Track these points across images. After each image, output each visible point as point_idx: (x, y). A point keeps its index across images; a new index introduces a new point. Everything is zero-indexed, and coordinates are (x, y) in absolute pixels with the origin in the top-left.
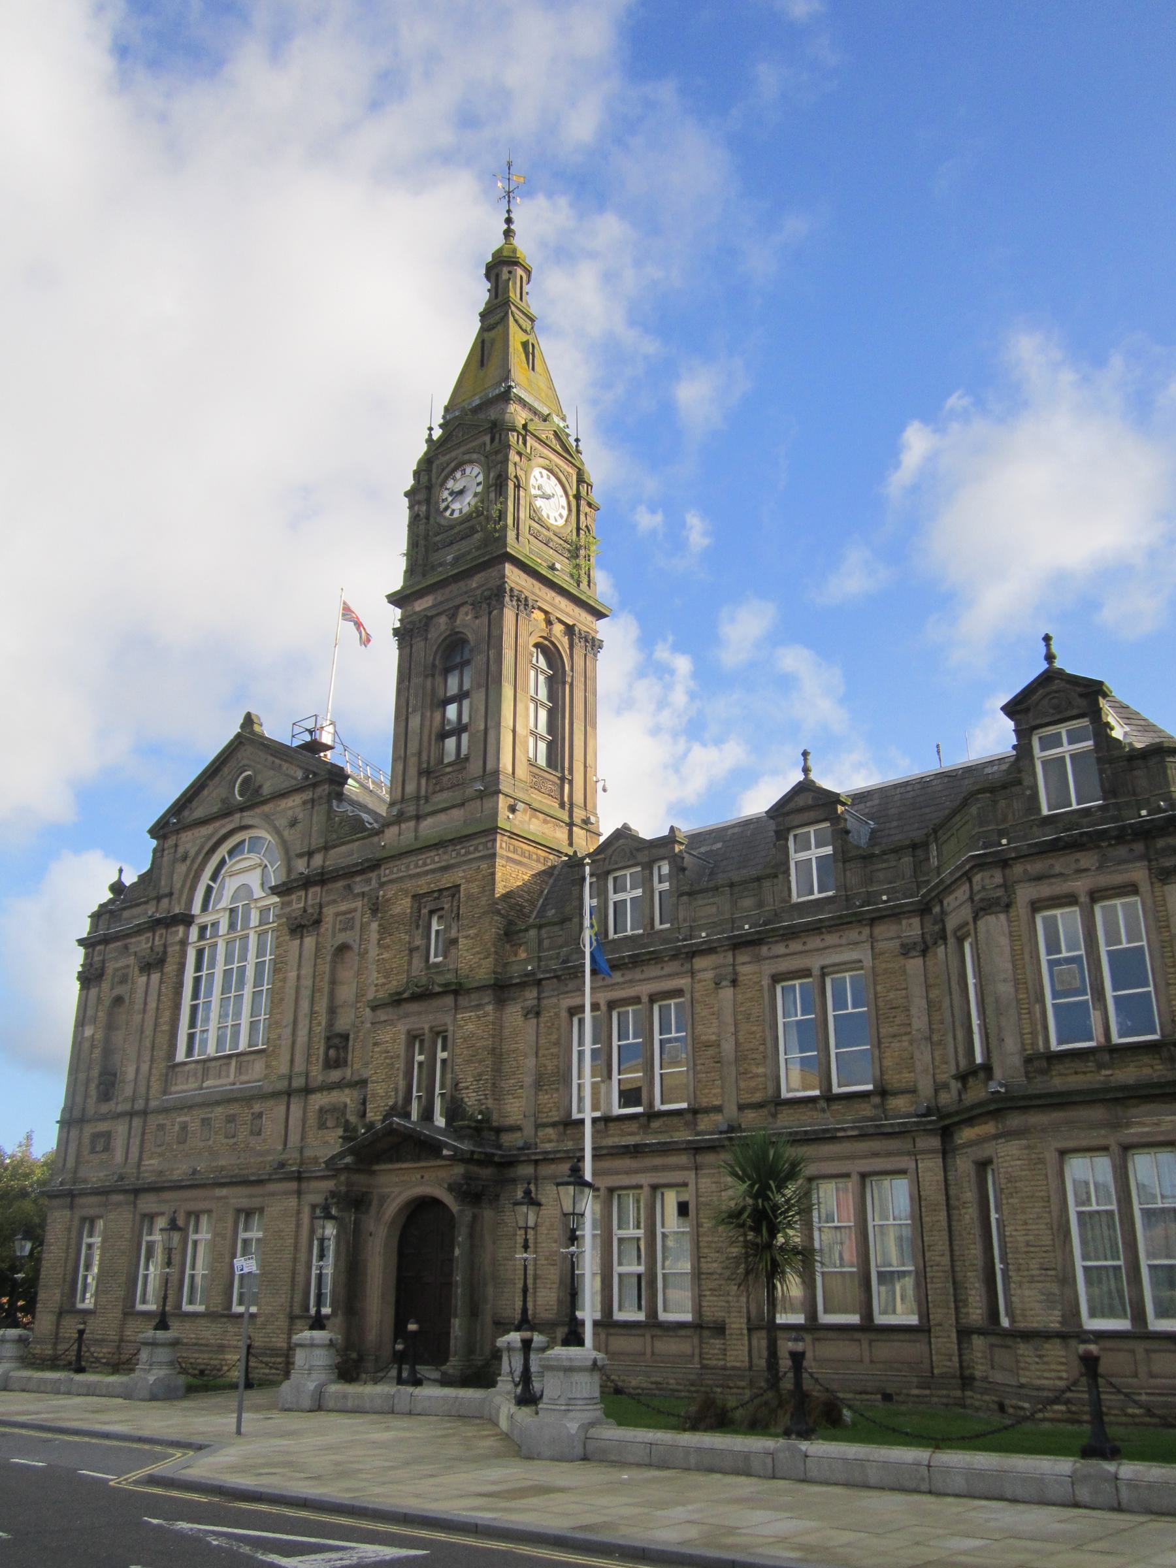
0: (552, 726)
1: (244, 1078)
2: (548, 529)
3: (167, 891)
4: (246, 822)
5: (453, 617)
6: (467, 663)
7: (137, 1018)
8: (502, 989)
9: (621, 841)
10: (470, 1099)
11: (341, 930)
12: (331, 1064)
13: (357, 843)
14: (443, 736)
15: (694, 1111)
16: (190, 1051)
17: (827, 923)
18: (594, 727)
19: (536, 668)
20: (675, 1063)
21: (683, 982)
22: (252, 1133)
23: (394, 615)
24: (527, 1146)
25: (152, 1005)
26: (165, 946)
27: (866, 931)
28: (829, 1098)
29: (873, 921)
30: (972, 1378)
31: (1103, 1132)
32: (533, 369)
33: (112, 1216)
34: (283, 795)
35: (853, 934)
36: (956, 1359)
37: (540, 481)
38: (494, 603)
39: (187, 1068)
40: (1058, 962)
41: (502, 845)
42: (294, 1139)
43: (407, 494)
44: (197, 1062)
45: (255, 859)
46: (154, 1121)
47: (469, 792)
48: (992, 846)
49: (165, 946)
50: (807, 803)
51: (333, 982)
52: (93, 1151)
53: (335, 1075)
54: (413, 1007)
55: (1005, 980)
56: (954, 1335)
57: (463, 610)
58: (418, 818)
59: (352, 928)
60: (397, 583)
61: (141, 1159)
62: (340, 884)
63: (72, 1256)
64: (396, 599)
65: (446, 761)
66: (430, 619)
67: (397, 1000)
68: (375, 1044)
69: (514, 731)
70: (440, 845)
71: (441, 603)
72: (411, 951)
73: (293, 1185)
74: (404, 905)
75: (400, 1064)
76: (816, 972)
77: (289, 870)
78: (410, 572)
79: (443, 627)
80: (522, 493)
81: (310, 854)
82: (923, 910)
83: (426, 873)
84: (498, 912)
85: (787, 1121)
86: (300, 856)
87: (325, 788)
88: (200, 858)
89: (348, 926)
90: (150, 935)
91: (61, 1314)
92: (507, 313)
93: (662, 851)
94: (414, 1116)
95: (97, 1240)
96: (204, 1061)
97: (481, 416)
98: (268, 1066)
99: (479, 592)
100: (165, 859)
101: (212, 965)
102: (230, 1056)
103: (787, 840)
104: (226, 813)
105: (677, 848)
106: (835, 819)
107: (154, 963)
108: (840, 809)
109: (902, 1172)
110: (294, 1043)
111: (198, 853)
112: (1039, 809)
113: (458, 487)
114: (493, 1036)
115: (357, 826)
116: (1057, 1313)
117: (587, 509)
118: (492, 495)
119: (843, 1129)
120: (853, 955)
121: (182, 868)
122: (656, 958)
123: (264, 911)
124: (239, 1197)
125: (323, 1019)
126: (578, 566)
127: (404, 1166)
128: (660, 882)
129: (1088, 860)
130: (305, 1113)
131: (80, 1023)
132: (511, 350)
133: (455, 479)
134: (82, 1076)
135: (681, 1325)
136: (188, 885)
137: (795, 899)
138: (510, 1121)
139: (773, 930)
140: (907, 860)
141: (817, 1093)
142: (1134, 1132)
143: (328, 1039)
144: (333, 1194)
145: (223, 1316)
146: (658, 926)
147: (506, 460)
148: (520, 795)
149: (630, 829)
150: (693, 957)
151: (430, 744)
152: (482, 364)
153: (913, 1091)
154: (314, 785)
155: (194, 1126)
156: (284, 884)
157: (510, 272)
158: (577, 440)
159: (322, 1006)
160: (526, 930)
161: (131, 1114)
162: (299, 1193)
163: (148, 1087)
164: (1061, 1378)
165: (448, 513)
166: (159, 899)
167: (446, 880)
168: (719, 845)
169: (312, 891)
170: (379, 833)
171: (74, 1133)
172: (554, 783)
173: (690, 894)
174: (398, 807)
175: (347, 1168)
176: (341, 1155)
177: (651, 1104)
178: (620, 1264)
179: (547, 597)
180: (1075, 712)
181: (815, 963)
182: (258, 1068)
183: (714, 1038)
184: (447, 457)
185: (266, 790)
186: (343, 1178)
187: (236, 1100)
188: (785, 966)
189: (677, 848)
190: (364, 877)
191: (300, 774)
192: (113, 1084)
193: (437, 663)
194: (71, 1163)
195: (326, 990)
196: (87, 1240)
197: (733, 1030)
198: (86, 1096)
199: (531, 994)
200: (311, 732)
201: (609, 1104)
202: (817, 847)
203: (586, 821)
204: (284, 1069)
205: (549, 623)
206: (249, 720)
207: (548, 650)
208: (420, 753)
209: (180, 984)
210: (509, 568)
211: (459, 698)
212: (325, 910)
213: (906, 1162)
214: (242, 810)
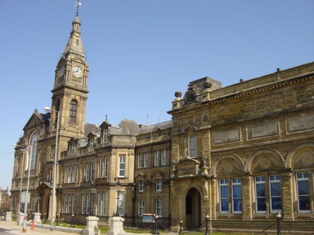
23: (52, 94)
34: (39, 125)
60: (52, 89)
64: (52, 91)
117: (87, 72)
205: (75, 96)
206: (35, 111)
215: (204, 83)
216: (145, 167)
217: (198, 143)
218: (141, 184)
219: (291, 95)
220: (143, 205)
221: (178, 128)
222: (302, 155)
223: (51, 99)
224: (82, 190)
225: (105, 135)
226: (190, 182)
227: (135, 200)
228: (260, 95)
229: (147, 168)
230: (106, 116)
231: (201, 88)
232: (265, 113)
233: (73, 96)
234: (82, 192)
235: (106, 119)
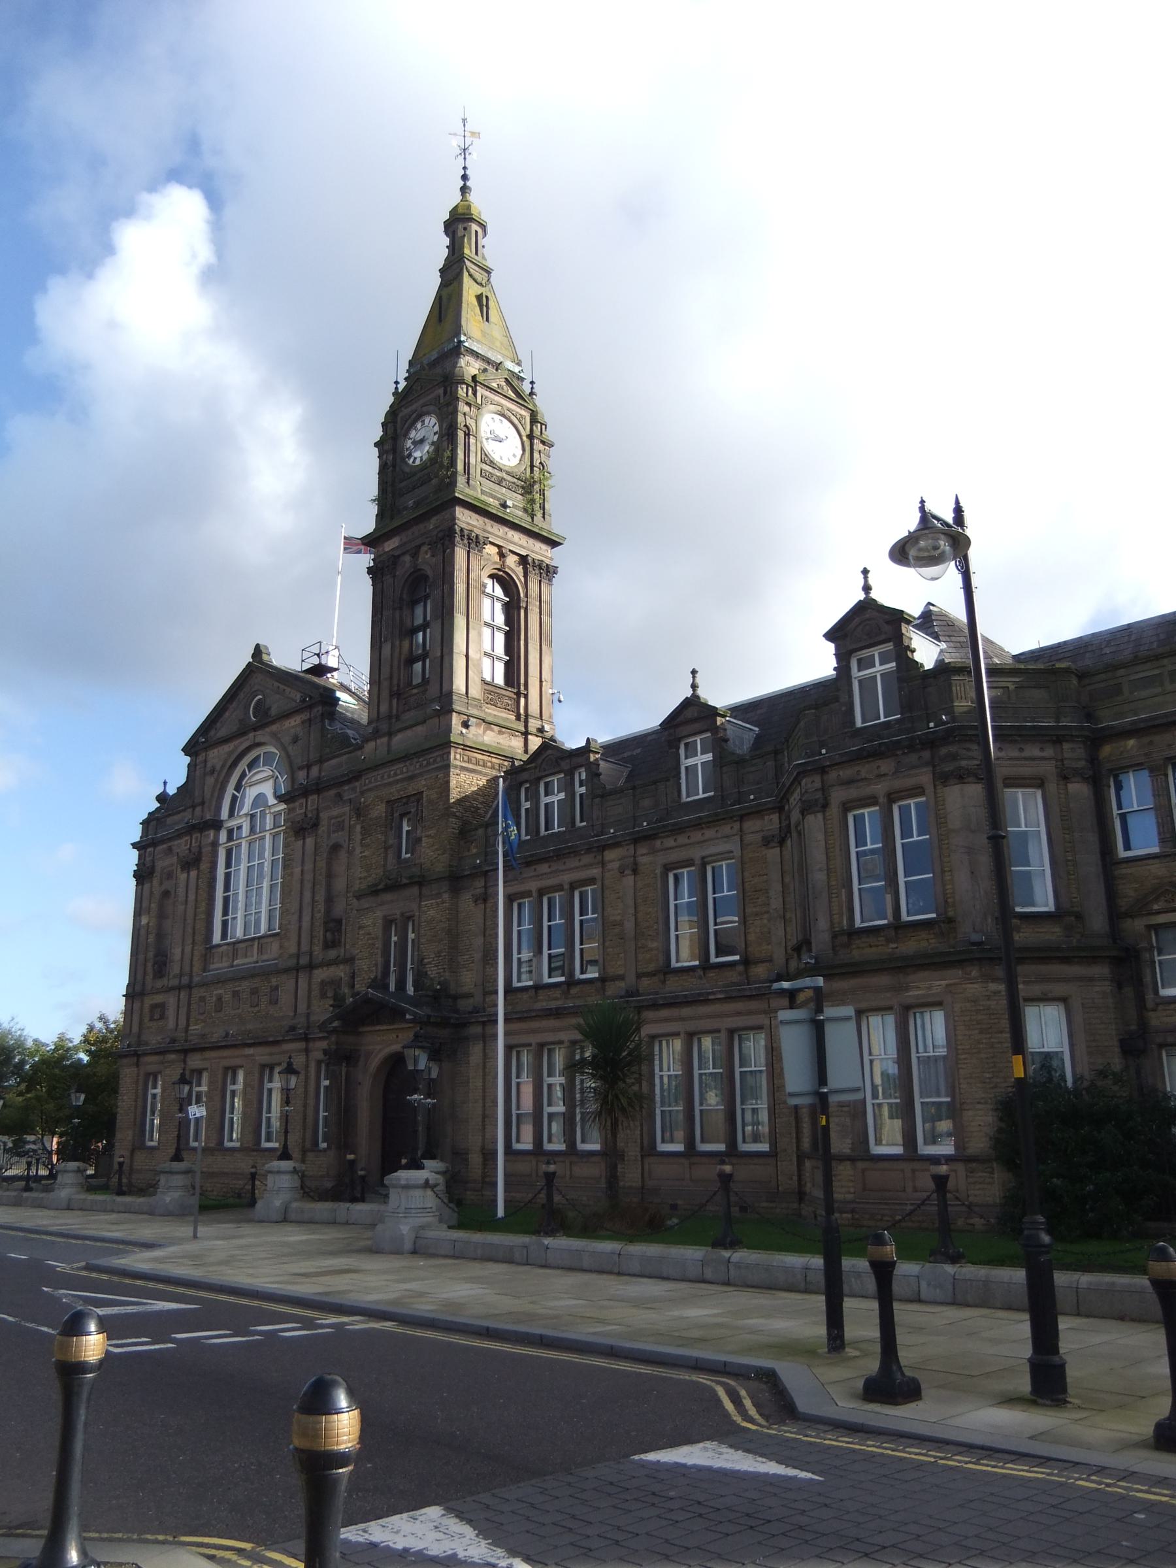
1: (265, 957)
2: (501, 470)
3: (198, 800)
4: (259, 739)
5: (415, 555)
6: (427, 597)
7: (181, 908)
8: (456, 880)
9: (549, 752)
10: (432, 971)
11: (334, 832)
12: (328, 945)
13: (345, 757)
14: (411, 661)
15: (603, 980)
16: (224, 935)
17: (705, 820)
18: (550, 645)
19: (492, 597)
20: (591, 939)
21: (595, 872)
22: (271, 1003)
24: (476, 1010)
25: (192, 897)
26: (200, 847)
27: (737, 826)
28: (706, 966)
29: (742, 818)
30: (805, 1193)
31: (888, 995)
32: (487, 320)
33: (168, 1071)
34: (287, 715)
35: (726, 829)
36: (795, 1178)
37: (493, 426)
38: (447, 543)
39: (221, 949)
40: (865, 853)
41: (456, 757)
42: (302, 1007)
43: (376, 445)
44: (228, 944)
45: (267, 772)
46: (197, 993)
47: (429, 711)
48: (813, 755)
49: (200, 847)
50: (693, 715)
52: (152, 1019)
53: (332, 954)
54: (388, 897)
55: (820, 870)
56: (795, 1159)
57: (425, 548)
58: (390, 734)
59: (343, 829)
61: (188, 1025)
62: (332, 792)
63: (140, 1103)
64: (370, 542)
65: (415, 682)
66: (399, 556)
67: (374, 891)
68: (360, 928)
69: (467, 656)
70: (406, 757)
71: (405, 543)
72: (386, 849)
73: (302, 1045)
74: (379, 810)
75: (379, 944)
76: (698, 862)
77: (293, 779)
78: (380, 517)
79: (408, 565)
80: (472, 440)
81: (308, 767)
82: (780, 809)
83: (397, 782)
84: (454, 815)
85: (673, 986)
86: (301, 768)
88: (225, 771)
89: (340, 827)
90: (188, 838)
91: (132, 1152)
92: (462, 270)
93: (580, 760)
94: (392, 987)
95: (158, 1091)
96: (234, 943)
97: (438, 370)
98: (281, 947)
99: (435, 533)
100: (198, 773)
101: (238, 863)
102: (253, 939)
103: (678, 748)
104: (241, 733)
105: (592, 757)
106: (715, 729)
107: (191, 862)
108: (719, 720)
109: (759, 1028)
110: (300, 928)
111: (223, 766)
112: (853, 722)
113: (419, 437)
114: (449, 920)
115: (344, 741)
116: (849, 1141)
118: (445, 444)
119: (713, 993)
120: (722, 847)
121: (210, 781)
122: (574, 852)
123: (276, 816)
124: (261, 1055)
125: (321, 907)
127: (385, 1027)
128: (581, 786)
130: (310, 984)
131: (138, 913)
132: (464, 305)
133: (416, 429)
134: (141, 957)
135: (592, 1153)
136: (216, 794)
137: (684, 799)
138: (465, 989)
139: (664, 826)
140: (771, 763)
141: (697, 963)
143: (325, 923)
144: (325, 1052)
145: (254, 1150)
146: (578, 824)
147: (456, 411)
149: (555, 741)
150: (603, 850)
151: (399, 667)
152: (440, 320)
153: (771, 961)
154: (310, 707)
155: (227, 997)
156: (287, 793)
157: (465, 229)
158: (532, 383)
159: (321, 897)
160: (476, 829)
161: (179, 988)
162: (307, 1051)
163: (192, 965)
164: (849, 1193)
165: (411, 461)
166: (194, 807)
167: (411, 791)
168: (639, 751)
169: (310, 798)
170: (360, 747)
171: (137, 1005)
172: (510, 698)
173: (602, 796)
174: (374, 725)
175: (335, 1030)
176: (330, 1020)
177: (571, 973)
178: (549, 1105)
179: (498, 532)
180: (883, 637)
181: (697, 854)
182: (274, 948)
183: (618, 918)
184: (409, 409)
185: (273, 712)
186: (333, 1039)
187: (258, 975)
188: (674, 856)
189: (592, 757)
190: (351, 786)
191: (298, 697)
192: (165, 964)
193: (405, 596)
194: (135, 1029)
195: (324, 883)
196: (151, 1091)
197: (632, 911)
198: (145, 973)
199: (479, 883)
200: (318, 655)
201: (540, 975)
202: (702, 754)
204: (293, 950)
205: (502, 555)
206: (258, 651)
207: (504, 580)
208: (391, 678)
209: (213, 879)
211: (424, 627)
212: (321, 815)
213: (763, 1020)
214: (255, 730)
223: (367, 581)
224: (649, 1015)
233: (491, 550)
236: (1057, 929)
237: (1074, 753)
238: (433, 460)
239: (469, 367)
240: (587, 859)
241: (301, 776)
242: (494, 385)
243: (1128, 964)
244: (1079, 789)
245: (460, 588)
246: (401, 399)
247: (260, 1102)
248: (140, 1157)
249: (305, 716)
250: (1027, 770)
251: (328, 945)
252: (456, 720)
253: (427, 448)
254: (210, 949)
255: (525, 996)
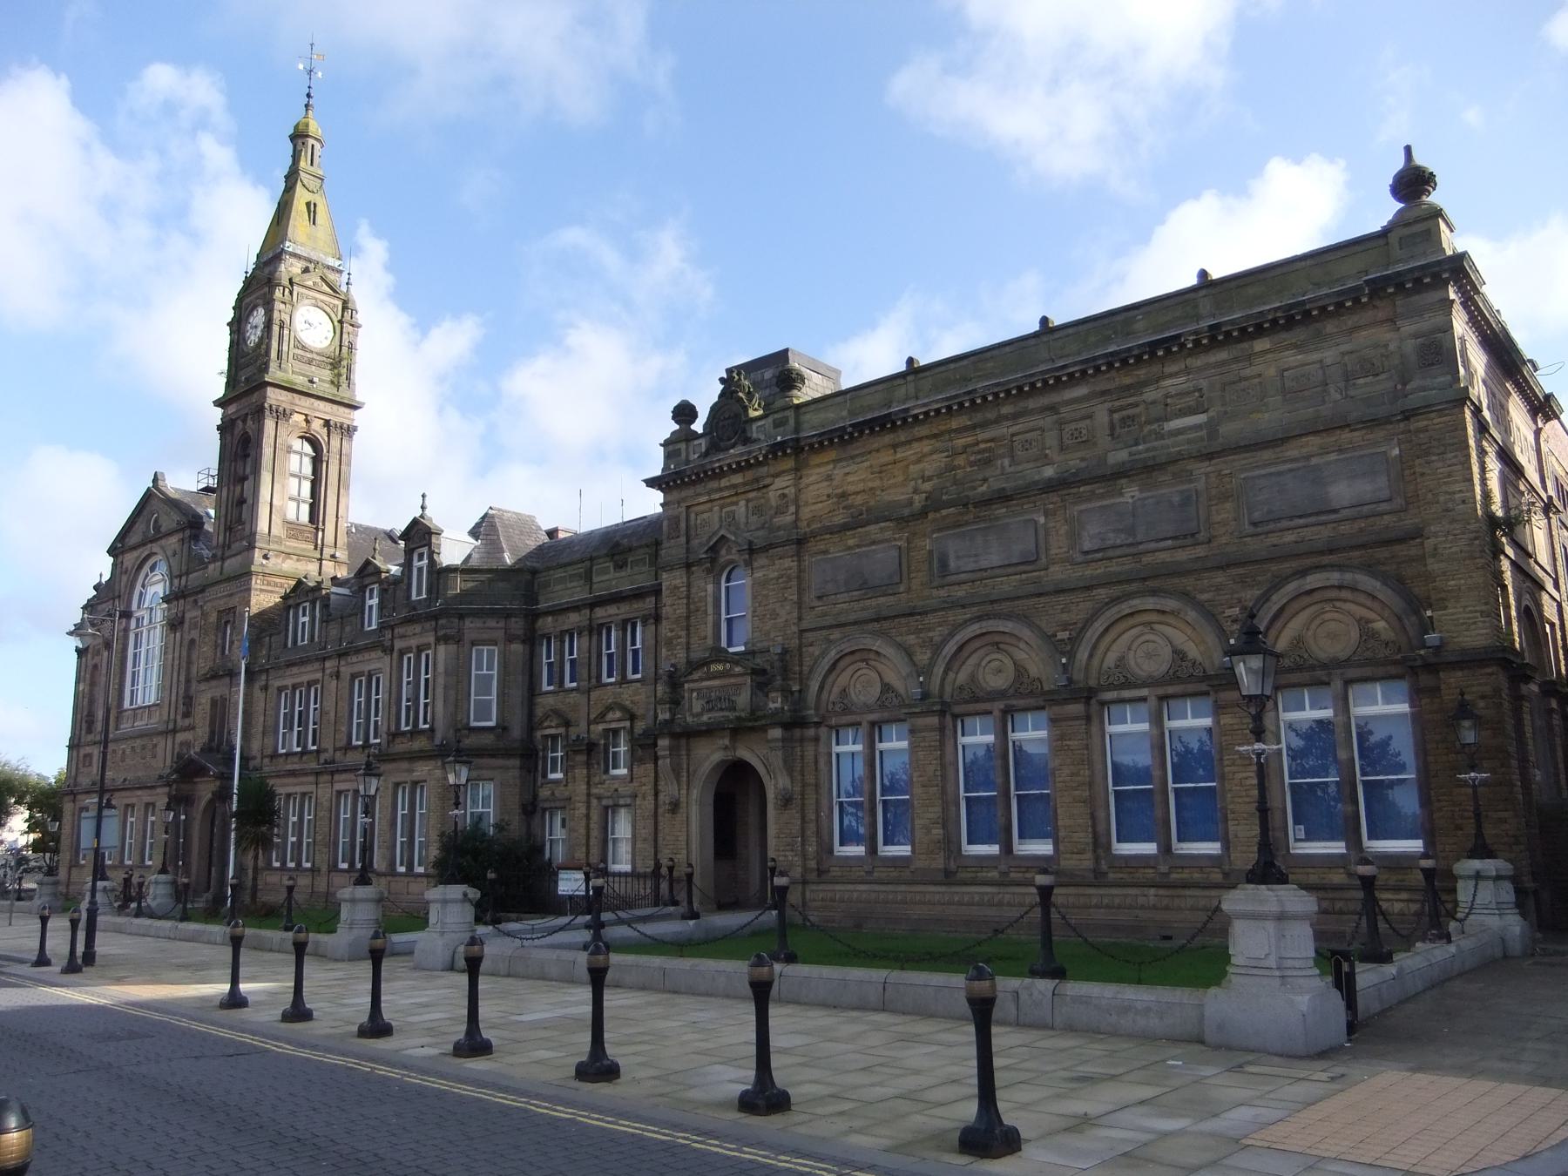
0: (314, 493)
5: (244, 421)
12: (186, 715)
15: (318, 752)
19: (301, 454)
21: (319, 675)
41: (256, 583)
51: (189, 663)
53: (187, 722)
54: (214, 683)
58: (223, 559)
60: (220, 392)
64: (218, 403)
70: (229, 579)
74: (213, 618)
80: (286, 332)
81: (180, 576)
87: (188, 532)
89: (194, 626)
97: (267, 270)
104: (143, 544)
106: (381, 582)
124: (145, 796)
125: (182, 686)
126: (339, 375)
129: (418, 628)
137: (367, 629)
142: (416, 775)
148: (272, 546)
154: (183, 530)
159: (182, 678)
175: (175, 781)
177: (305, 747)
181: (366, 668)
182: (155, 719)
185: (163, 529)
188: (356, 669)
199: (264, 677)
203: (333, 556)
204: (165, 718)
205: (307, 421)
206: (155, 480)
210: (269, 390)
215: (776, 373)
216: (569, 685)
217: (754, 598)
218: (554, 750)
219: (1090, 417)
220: (563, 826)
221: (683, 539)
222: (1125, 636)
223: (217, 435)
224: (337, 777)
225: (420, 570)
226: (727, 741)
227: (533, 812)
228: (979, 417)
229: (572, 690)
230: (423, 496)
231: (767, 392)
232: (995, 484)
233: (298, 419)
234: (338, 787)
235: (423, 508)
236: (492, 737)
237: (517, 625)
238: (258, 345)
239: (289, 268)
240: (317, 665)
241: (176, 582)
242: (310, 283)
243: (530, 757)
244: (517, 647)
245: (267, 451)
246: (248, 283)
247: (145, 831)
248: (74, 871)
249: (180, 536)
250: (485, 636)
251: (186, 715)
252: (258, 554)
253: (259, 333)
254: (121, 711)
255: (281, 760)
